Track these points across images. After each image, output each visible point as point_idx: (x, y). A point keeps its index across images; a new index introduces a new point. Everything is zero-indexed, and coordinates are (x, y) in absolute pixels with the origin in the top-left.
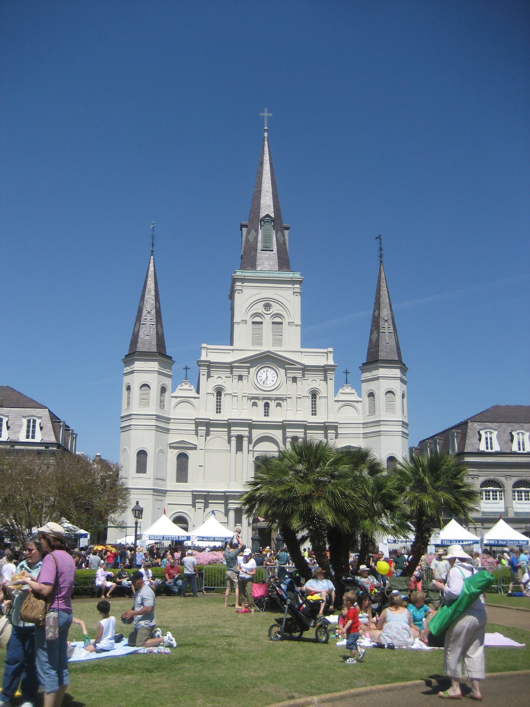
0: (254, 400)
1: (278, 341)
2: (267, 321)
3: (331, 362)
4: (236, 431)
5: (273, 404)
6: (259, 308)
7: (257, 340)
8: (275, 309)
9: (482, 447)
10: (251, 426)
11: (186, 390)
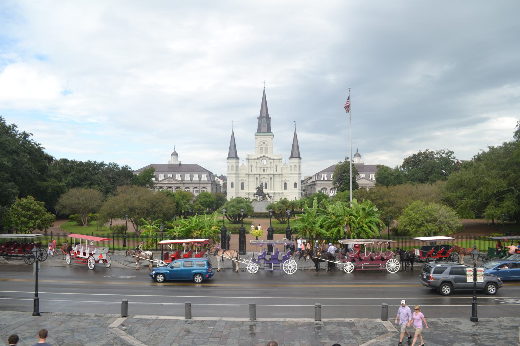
0: (260, 168)
1: (267, 152)
2: (264, 146)
4: (256, 176)
6: (262, 143)
8: (266, 143)
9: (322, 179)
10: (260, 175)
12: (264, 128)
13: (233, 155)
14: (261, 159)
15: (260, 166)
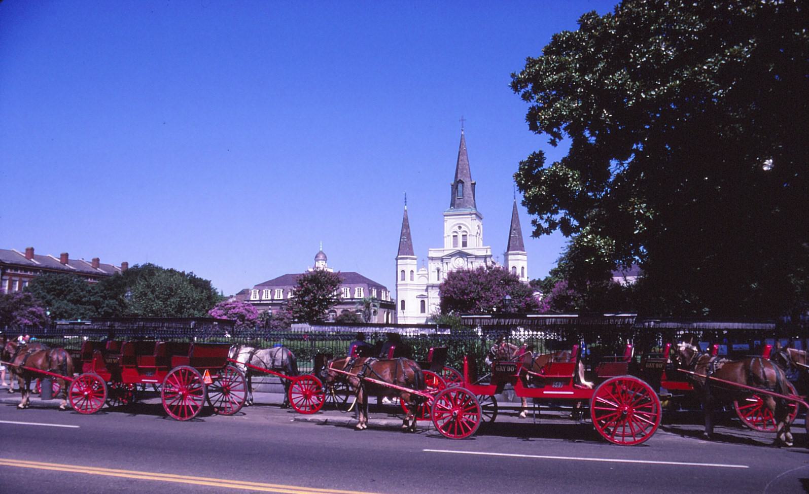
1: (465, 244)
3: (489, 253)
6: (456, 229)
7: (455, 244)
8: (464, 228)
11: (423, 271)
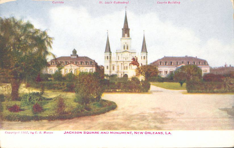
1: (127, 48)
5: (127, 58)
6: (125, 43)
8: (127, 43)
12: (126, 35)
13: (108, 49)
14: (124, 53)
15: (124, 56)
